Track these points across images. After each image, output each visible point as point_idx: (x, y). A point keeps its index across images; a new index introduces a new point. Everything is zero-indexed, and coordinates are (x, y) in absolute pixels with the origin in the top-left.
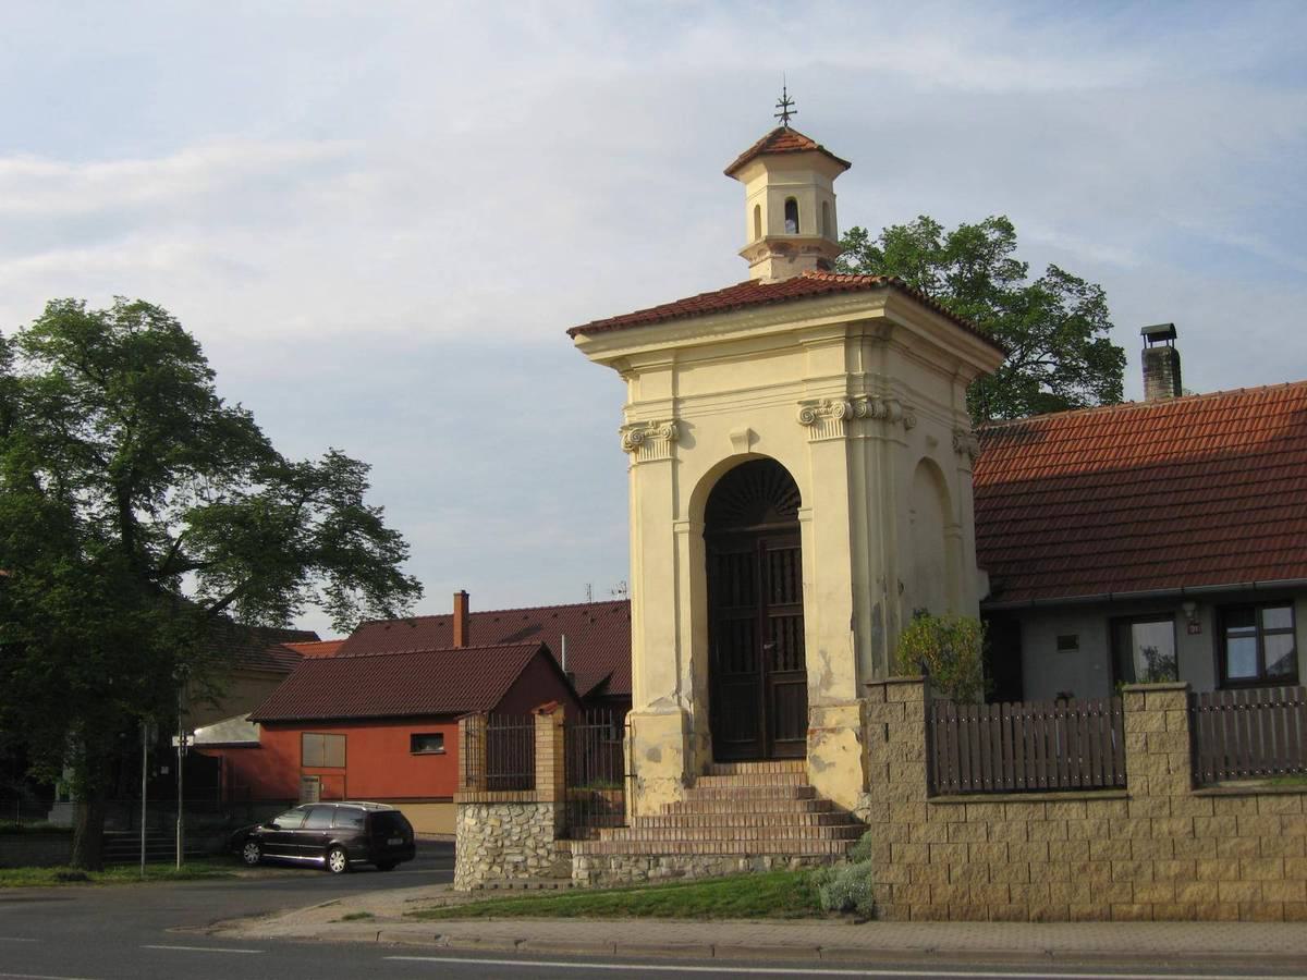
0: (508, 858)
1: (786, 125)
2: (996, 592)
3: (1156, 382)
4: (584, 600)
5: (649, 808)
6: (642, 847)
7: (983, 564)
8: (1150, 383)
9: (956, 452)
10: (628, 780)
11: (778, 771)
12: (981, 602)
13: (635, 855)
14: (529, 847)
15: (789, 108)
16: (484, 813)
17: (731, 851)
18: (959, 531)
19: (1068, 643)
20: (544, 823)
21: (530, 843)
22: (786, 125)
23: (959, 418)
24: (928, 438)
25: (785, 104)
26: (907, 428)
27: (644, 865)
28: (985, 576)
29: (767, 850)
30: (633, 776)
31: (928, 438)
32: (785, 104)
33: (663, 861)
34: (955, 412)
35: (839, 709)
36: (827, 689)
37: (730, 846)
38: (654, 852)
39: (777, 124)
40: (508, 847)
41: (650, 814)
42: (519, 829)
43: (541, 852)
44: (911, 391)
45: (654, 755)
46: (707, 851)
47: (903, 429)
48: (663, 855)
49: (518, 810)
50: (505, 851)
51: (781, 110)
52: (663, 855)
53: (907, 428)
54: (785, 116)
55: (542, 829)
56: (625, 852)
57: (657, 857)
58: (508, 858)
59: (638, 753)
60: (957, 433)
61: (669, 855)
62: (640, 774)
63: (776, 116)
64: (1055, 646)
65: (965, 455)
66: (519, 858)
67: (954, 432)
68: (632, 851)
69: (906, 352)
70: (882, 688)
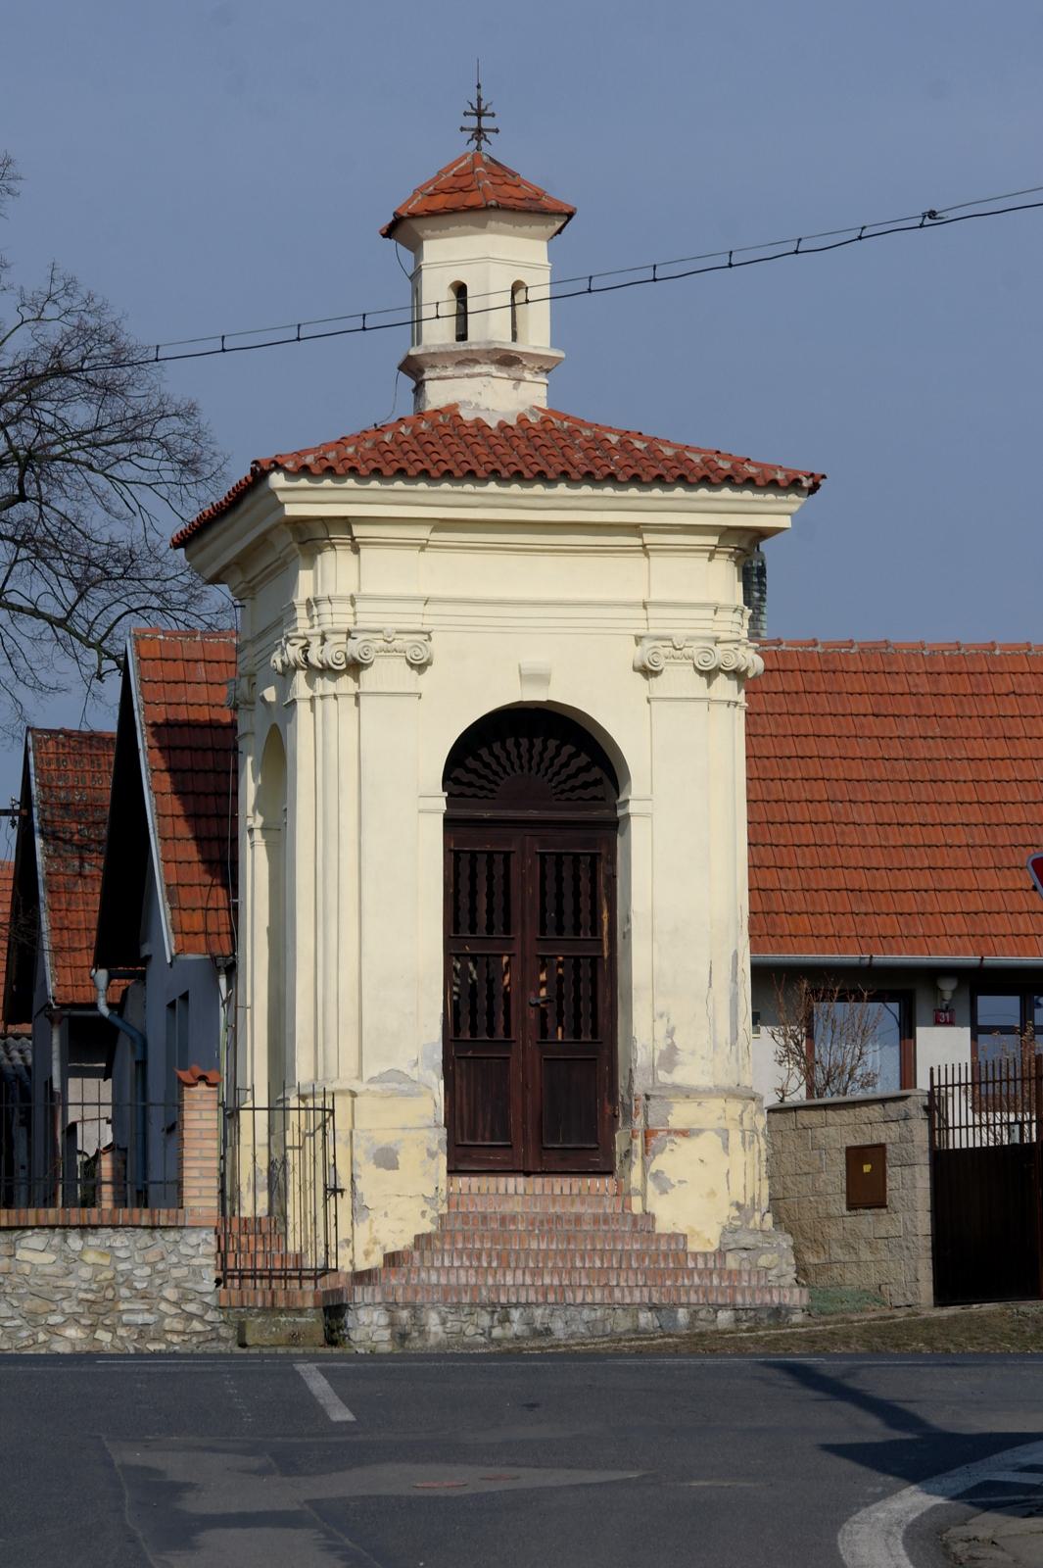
0: (125, 1318)
1: (478, 148)
5: (376, 1242)
6: (484, 1292)
11: (566, 1191)
13: (472, 1305)
15: (486, 123)
16: (75, 1242)
17: (628, 1300)
20: (196, 1262)
22: (478, 148)
25: (479, 114)
27: (485, 1320)
29: (684, 1299)
33: (515, 1314)
36: (669, 1072)
38: (503, 1300)
40: (127, 1299)
42: (147, 1270)
43: (191, 1308)
45: (387, 1159)
46: (589, 1299)
48: (517, 1305)
50: (122, 1306)
51: (472, 122)
52: (517, 1305)
54: (479, 133)
55: (196, 1272)
56: (455, 1300)
57: (507, 1307)
59: (359, 1155)
61: (528, 1304)
63: (462, 129)
66: (149, 1318)
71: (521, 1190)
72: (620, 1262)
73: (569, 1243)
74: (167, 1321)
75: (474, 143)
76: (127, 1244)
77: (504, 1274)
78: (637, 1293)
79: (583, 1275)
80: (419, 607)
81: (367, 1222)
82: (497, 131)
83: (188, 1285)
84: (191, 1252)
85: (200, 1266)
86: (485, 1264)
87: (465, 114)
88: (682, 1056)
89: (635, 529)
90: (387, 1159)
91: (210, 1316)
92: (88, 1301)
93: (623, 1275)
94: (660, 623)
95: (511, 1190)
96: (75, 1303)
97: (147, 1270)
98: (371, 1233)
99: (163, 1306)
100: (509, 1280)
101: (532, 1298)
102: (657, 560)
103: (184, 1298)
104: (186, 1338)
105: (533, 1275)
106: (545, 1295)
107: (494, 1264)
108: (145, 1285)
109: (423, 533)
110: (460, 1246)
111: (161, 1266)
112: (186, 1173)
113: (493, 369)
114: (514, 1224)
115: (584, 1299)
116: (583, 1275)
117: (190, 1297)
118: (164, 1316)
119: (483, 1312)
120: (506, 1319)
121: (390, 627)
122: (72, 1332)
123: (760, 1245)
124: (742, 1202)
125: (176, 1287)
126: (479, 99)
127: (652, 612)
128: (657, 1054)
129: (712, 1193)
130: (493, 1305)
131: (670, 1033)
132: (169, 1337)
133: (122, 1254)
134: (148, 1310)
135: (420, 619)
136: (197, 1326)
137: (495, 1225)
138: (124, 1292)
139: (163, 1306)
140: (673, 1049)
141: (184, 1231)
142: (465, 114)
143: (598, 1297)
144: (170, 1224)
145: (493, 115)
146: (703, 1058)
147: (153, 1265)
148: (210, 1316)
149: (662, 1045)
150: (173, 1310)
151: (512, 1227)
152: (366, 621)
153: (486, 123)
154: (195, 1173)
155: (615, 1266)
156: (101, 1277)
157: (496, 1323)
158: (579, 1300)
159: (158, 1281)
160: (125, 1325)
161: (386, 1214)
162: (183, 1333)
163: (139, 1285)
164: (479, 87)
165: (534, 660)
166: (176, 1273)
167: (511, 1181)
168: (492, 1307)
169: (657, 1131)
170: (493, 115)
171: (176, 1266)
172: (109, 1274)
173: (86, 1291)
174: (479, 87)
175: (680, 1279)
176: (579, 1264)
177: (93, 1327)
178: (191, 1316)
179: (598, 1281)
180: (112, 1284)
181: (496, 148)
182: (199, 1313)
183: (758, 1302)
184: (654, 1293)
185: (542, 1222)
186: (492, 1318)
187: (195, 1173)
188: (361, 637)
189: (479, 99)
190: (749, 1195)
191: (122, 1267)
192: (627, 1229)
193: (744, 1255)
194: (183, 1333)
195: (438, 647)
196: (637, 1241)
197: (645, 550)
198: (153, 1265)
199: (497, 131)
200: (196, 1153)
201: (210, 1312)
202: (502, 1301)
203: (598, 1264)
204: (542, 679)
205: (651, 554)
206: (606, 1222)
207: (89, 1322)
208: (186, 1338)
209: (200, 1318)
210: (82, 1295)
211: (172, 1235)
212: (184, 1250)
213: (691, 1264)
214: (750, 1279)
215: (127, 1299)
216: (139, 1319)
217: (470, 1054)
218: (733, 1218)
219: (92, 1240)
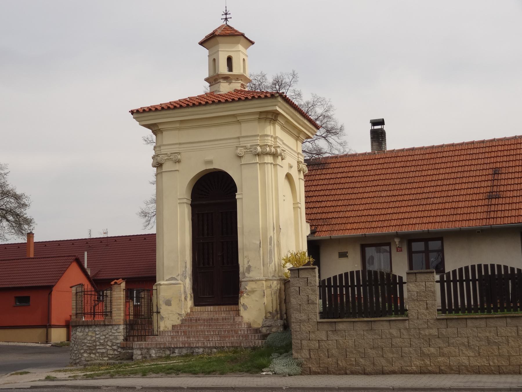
0: (98, 351)
1: (226, 23)
2: (313, 232)
3: (377, 144)
4: (86, 236)
5: (166, 327)
6: (167, 344)
7: (308, 220)
8: (374, 144)
9: (298, 171)
10: (155, 314)
11: (225, 310)
12: (307, 237)
13: (164, 348)
14: (108, 346)
15: (228, 16)
16: (87, 330)
17: (209, 346)
18: (299, 205)
19: (343, 255)
20: (116, 334)
21: (109, 343)
22: (226, 23)
23: (300, 156)
24: (289, 164)
25: (226, 14)
26: (282, 159)
27: (168, 352)
28: (309, 225)
30: (158, 312)
31: (289, 164)
32: (226, 14)
33: (177, 351)
34: (298, 154)
35: (254, 283)
36: (249, 273)
37: (208, 343)
38: (173, 346)
39: (222, 23)
41: (166, 329)
42: (104, 337)
43: (115, 347)
44: (284, 143)
45: (168, 303)
46: (197, 346)
47: (281, 160)
48: (177, 348)
49: (103, 329)
50: (97, 347)
51: (224, 17)
52: (177, 348)
53: (282, 159)
54: (226, 19)
57: (174, 348)
58: (98, 351)
59: (161, 302)
60: (299, 163)
61: (180, 348)
62: (161, 311)
63: (222, 19)
64: (337, 256)
65: (302, 172)
66: (104, 351)
67: (298, 162)
68: (162, 346)
69: (283, 128)
70: (297, 271)
71: (212, 310)
72: (219, 333)
73: (209, 327)
74: (109, 351)
75: (225, 22)
76: (99, 330)
77: (179, 338)
78: (212, 344)
79: (202, 338)
80: (177, 146)
81: (163, 322)
82: (231, 18)
83: (114, 341)
84: (115, 332)
85: (117, 336)
86: (180, 334)
87: (222, 15)
88: (252, 269)
89: (234, 116)
90: (168, 303)
91: (119, 350)
92: (89, 346)
93: (214, 337)
94: (244, 142)
95: (209, 310)
96: (86, 347)
97: (104, 337)
98: (165, 324)
99: (108, 347)
100: (181, 340)
101: (181, 346)
102: (243, 125)
103: (113, 345)
104: (113, 356)
105: (188, 338)
106: (185, 344)
107: (182, 334)
108: (103, 341)
109: (178, 125)
110: (179, 329)
111: (107, 336)
112: (113, 309)
113: (222, 81)
114: (199, 321)
115: (196, 345)
116: (202, 338)
117: (114, 344)
118: (108, 350)
119: (167, 350)
120: (174, 352)
121: (169, 153)
122: (85, 355)
123: (272, 325)
124: (271, 311)
125: (111, 342)
126: (226, 10)
127: (241, 140)
128: (245, 268)
129: (260, 309)
130: (170, 348)
131: (248, 262)
132: (109, 356)
133: (97, 333)
134: (104, 348)
135: (178, 149)
136: (116, 353)
137: (194, 322)
138: (98, 343)
139: (108, 347)
140: (249, 267)
141: (113, 326)
142: (222, 15)
143: (200, 345)
144: (109, 324)
145: (230, 14)
146: (258, 269)
147: (105, 335)
148: (119, 350)
149: (246, 266)
150: (110, 348)
151: (199, 322)
152: (163, 152)
153: (228, 16)
154: (115, 309)
155: (217, 334)
156: (92, 339)
157: (171, 353)
158: (195, 346)
159: (106, 340)
160: (98, 353)
161: (168, 319)
162: (113, 355)
163: (101, 341)
164: (226, 7)
165: (209, 158)
166: (111, 338)
167: (209, 307)
168: (169, 348)
169: (243, 291)
170: (230, 14)
171: (111, 335)
172: (94, 338)
173: (89, 343)
174: (226, 7)
175: (230, 338)
176: (207, 333)
177: (90, 353)
178: (114, 350)
179: (206, 339)
180: (95, 341)
181: (230, 23)
182: (116, 349)
183: (248, 345)
184: (217, 343)
185: (207, 320)
186: (170, 352)
187: (115, 309)
188: (161, 156)
189: (226, 10)
190: (275, 309)
191: (97, 336)
192: (232, 321)
193: (268, 328)
194: (113, 355)
195: (183, 157)
196: (229, 326)
197: (239, 122)
198: (105, 335)
199: (231, 18)
200: (115, 304)
201: (119, 349)
202: (172, 347)
203: (212, 333)
204: (210, 162)
205: (241, 123)
206: (226, 319)
207: (89, 352)
208: (113, 356)
209: (117, 350)
210: (88, 345)
211: (110, 327)
212: (113, 331)
213: (240, 333)
214: (252, 338)
215: (98, 345)
216: (101, 351)
217: (202, 271)
218: (269, 317)
219: (91, 329)
